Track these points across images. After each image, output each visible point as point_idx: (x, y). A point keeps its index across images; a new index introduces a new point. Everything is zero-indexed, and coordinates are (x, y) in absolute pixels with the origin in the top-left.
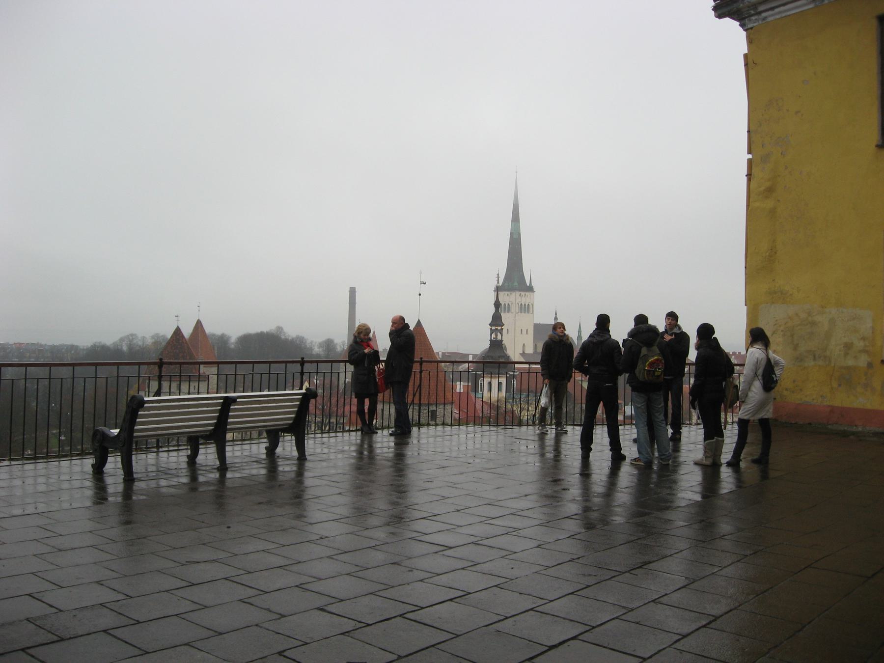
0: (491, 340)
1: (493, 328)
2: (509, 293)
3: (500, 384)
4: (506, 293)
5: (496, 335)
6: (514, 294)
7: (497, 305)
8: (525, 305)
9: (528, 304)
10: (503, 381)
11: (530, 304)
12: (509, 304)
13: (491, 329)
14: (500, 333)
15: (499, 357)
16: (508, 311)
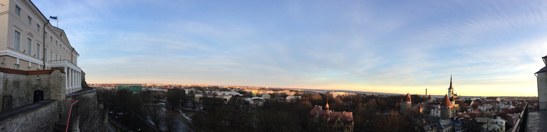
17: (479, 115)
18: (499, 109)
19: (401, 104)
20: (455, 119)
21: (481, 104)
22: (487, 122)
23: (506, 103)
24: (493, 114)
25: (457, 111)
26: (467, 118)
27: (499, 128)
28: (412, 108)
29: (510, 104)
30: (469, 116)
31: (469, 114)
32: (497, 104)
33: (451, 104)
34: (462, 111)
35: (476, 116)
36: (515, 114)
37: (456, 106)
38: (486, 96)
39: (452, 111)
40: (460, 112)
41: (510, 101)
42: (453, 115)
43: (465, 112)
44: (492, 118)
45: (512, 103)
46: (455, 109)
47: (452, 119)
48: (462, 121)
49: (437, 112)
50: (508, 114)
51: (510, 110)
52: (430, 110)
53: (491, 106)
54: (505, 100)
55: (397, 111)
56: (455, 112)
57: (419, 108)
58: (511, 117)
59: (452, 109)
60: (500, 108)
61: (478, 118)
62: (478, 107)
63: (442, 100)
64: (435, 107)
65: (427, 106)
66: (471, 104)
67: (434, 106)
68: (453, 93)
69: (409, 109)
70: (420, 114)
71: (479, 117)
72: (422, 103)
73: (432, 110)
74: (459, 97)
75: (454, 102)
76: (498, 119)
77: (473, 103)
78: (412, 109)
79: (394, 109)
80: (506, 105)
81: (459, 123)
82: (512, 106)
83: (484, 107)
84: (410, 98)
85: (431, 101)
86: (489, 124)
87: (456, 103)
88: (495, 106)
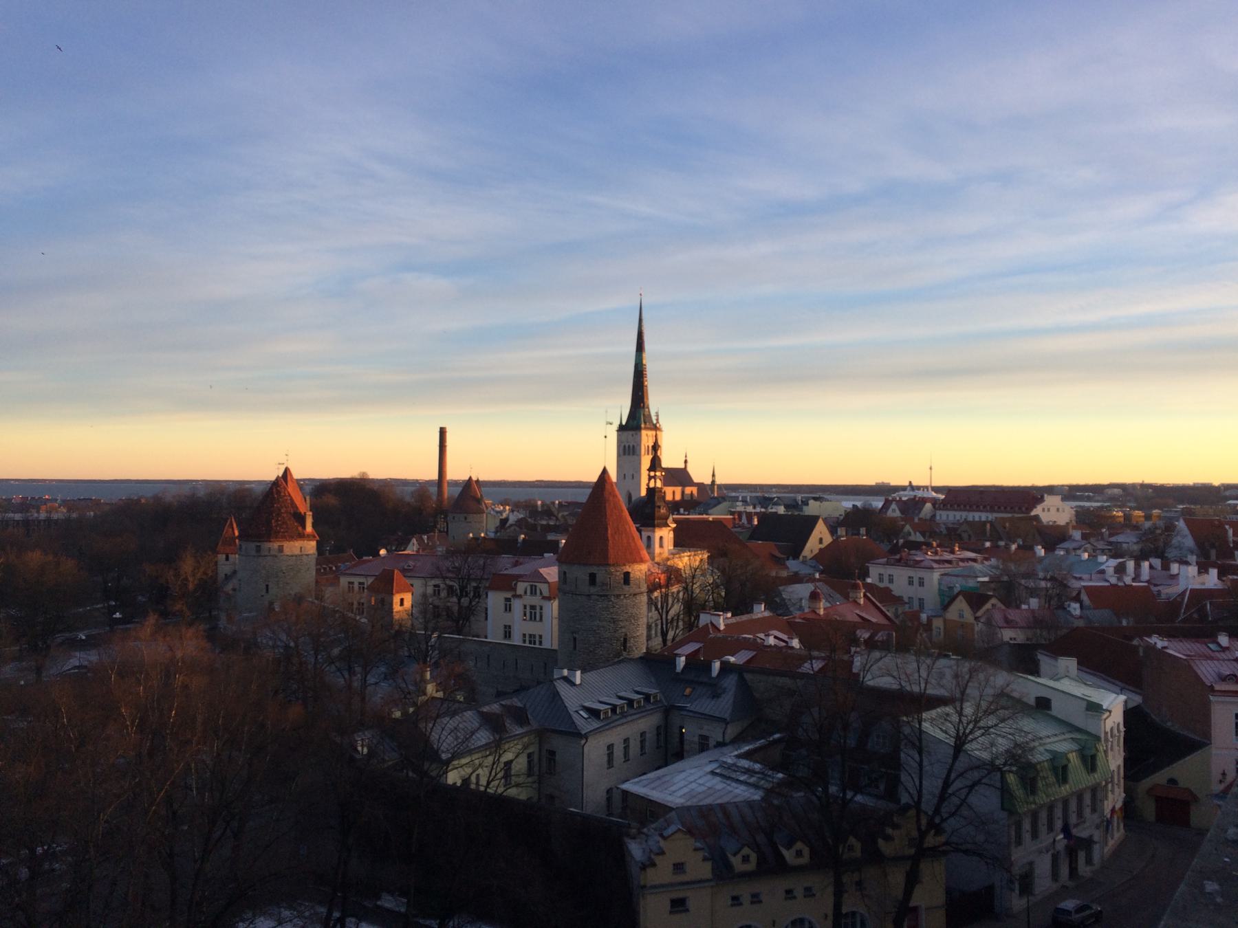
1: (652, 474)
2: (634, 432)
4: (631, 433)
5: (655, 482)
6: (639, 433)
12: (633, 446)
13: (649, 475)
17: (880, 637)
18: (1060, 593)
19: (224, 568)
20: (681, 662)
21: (895, 550)
22: (958, 695)
23: (1128, 540)
24: (1007, 635)
25: (692, 607)
26: (783, 652)
27: (1064, 745)
28: (329, 592)
29: (1171, 554)
30: (795, 643)
31: (792, 628)
32: (1040, 551)
33: (642, 544)
34: (739, 605)
35: (855, 641)
36: (1224, 640)
37: (686, 561)
38: (938, 483)
39: (651, 602)
40: (720, 607)
41: (1170, 528)
42: (664, 635)
43: (760, 610)
44: (996, 664)
45: (1189, 542)
46: (674, 589)
47: (658, 663)
48: (742, 680)
49: (534, 614)
50: (1159, 642)
51: (1173, 605)
52: (477, 595)
53: (982, 571)
54: (1118, 513)
55: (190, 624)
56: (676, 609)
57: (385, 585)
58: (1184, 668)
59: (653, 587)
60: (1076, 585)
61: (876, 654)
62: (865, 574)
63: (572, 521)
64: (518, 578)
65: (448, 564)
66: (812, 546)
67: (505, 564)
68: (655, 464)
69: (299, 599)
70: (399, 633)
71: (885, 646)
72: (412, 548)
73: (494, 600)
74: (712, 495)
75: (665, 535)
76: (1056, 678)
77: (828, 539)
78: (320, 597)
79: (164, 614)
80: (1131, 565)
81: (716, 696)
82: (1192, 570)
83: (916, 574)
84: (303, 507)
85: (486, 527)
86: (969, 709)
87: (683, 540)
88: (1023, 569)
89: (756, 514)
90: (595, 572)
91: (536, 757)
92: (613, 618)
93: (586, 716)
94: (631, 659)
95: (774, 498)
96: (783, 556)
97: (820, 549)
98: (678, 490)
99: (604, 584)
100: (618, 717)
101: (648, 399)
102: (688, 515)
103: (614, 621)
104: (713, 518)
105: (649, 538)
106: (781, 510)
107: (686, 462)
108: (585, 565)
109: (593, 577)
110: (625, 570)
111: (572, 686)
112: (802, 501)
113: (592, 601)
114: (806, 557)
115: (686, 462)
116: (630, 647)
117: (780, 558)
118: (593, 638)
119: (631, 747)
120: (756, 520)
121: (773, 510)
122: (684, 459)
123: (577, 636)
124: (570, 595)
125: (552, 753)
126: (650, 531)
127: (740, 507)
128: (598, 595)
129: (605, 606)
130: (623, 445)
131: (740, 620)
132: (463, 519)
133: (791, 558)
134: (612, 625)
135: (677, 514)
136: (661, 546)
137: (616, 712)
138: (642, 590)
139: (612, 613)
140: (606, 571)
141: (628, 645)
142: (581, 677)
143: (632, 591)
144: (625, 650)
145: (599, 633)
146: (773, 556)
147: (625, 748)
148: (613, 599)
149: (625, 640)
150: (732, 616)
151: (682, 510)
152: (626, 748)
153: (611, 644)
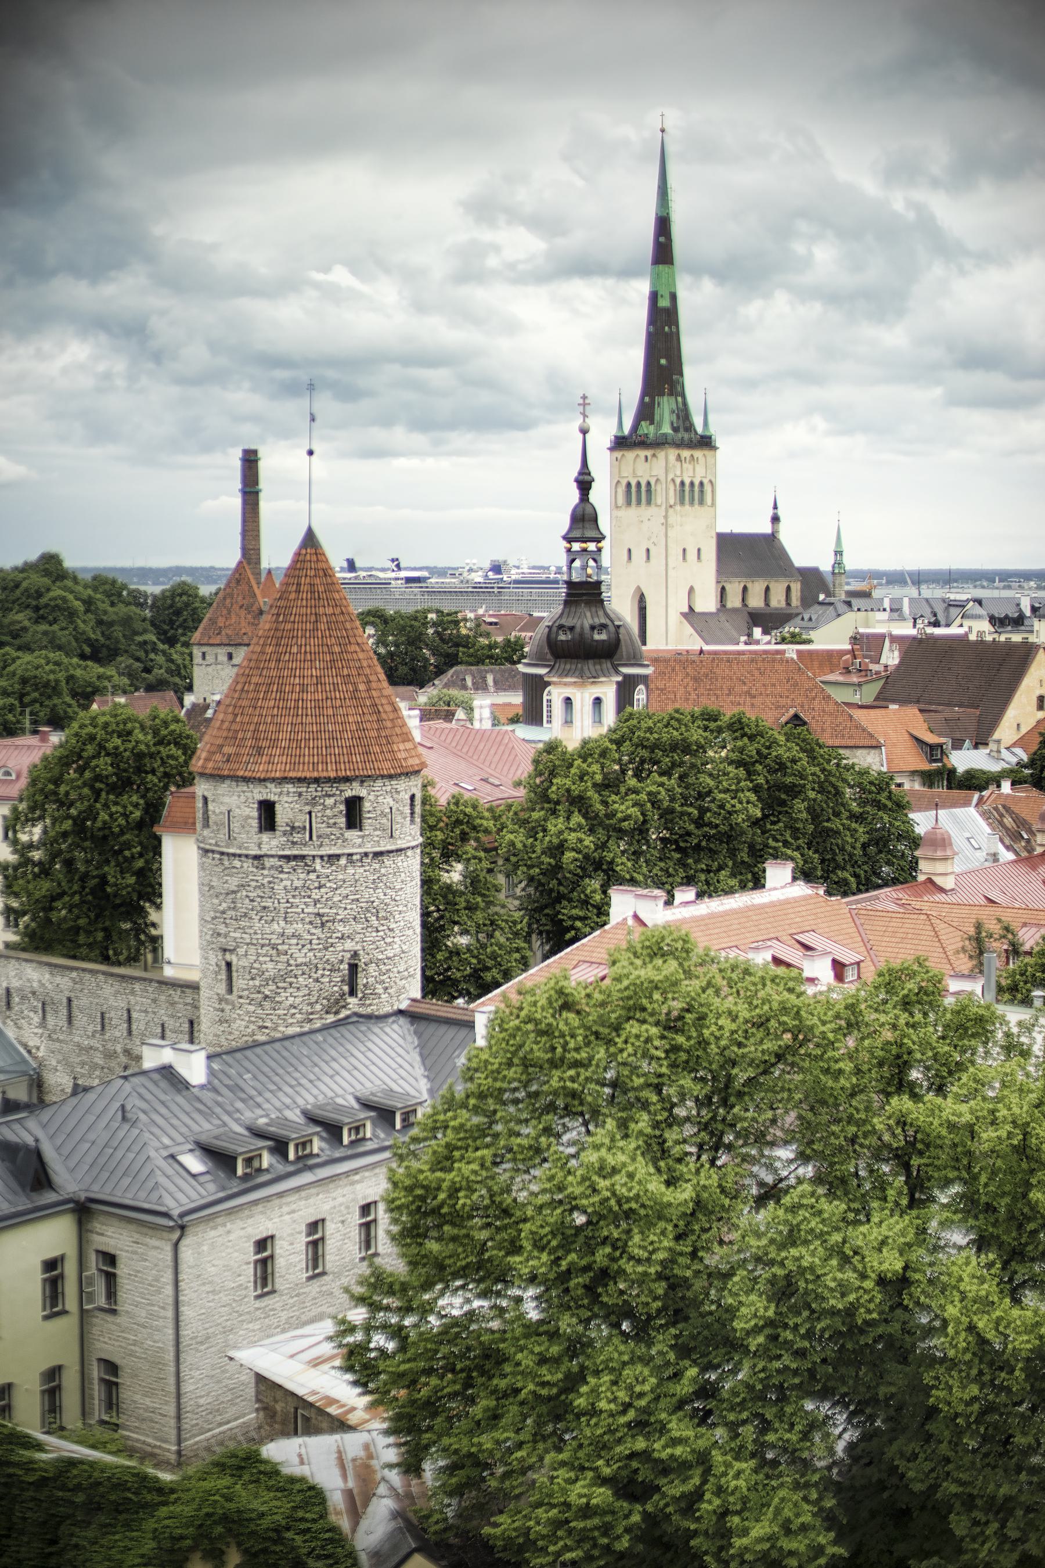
0: (570, 584)
1: (576, 546)
2: (649, 453)
3: (598, 701)
4: (642, 453)
5: (584, 567)
6: (661, 454)
7: (584, 485)
8: (692, 484)
9: (701, 484)
10: (605, 694)
11: (706, 481)
12: (649, 484)
13: (569, 550)
14: (595, 560)
15: (593, 628)
16: (649, 502)
89: (894, 639)
90: (273, 798)
91: (70, 1269)
92: (318, 914)
93: (195, 1163)
94: (369, 1017)
95: (968, 601)
96: (942, 740)
97: (1038, 722)
98: (756, 589)
99: (293, 828)
100: (291, 1168)
101: (681, 374)
102: (769, 643)
103: (322, 921)
104: (799, 652)
105: (568, 701)
106: (979, 629)
107: (775, 519)
108: (246, 780)
109: (267, 812)
110: (349, 793)
111: (179, 1091)
112: (1034, 610)
113: (266, 872)
114: (998, 742)
115: (775, 519)
116: (365, 986)
117: (932, 747)
118: (270, 965)
119: (328, 1242)
120: (896, 653)
121: (961, 631)
122: (770, 513)
123: (234, 959)
124: (217, 856)
125: (111, 1259)
126: (565, 684)
127: (879, 624)
128: (281, 857)
129: (297, 883)
130: (624, 482)
131: (721, 909)
132: (225, 659)
133: (967, 743)
134: (318, 931)
135: (746, 643)
136: (598, 718)
137: (285, 1155)
138: (401, 844)
139: (316, 902)
140: (300, 795)
141: (361, 981)
142: (209, 1067)
143: (370, 848)
144: (352, 992)
145: (286, 953)
146: (918, 740)
147: (315, 1244)
148: (318, 867)
149: (353, 968)
150: (700, 895)
151: (757, 632)
152: (316, 1247)
153: (317, 980)
